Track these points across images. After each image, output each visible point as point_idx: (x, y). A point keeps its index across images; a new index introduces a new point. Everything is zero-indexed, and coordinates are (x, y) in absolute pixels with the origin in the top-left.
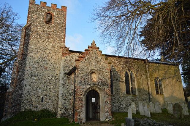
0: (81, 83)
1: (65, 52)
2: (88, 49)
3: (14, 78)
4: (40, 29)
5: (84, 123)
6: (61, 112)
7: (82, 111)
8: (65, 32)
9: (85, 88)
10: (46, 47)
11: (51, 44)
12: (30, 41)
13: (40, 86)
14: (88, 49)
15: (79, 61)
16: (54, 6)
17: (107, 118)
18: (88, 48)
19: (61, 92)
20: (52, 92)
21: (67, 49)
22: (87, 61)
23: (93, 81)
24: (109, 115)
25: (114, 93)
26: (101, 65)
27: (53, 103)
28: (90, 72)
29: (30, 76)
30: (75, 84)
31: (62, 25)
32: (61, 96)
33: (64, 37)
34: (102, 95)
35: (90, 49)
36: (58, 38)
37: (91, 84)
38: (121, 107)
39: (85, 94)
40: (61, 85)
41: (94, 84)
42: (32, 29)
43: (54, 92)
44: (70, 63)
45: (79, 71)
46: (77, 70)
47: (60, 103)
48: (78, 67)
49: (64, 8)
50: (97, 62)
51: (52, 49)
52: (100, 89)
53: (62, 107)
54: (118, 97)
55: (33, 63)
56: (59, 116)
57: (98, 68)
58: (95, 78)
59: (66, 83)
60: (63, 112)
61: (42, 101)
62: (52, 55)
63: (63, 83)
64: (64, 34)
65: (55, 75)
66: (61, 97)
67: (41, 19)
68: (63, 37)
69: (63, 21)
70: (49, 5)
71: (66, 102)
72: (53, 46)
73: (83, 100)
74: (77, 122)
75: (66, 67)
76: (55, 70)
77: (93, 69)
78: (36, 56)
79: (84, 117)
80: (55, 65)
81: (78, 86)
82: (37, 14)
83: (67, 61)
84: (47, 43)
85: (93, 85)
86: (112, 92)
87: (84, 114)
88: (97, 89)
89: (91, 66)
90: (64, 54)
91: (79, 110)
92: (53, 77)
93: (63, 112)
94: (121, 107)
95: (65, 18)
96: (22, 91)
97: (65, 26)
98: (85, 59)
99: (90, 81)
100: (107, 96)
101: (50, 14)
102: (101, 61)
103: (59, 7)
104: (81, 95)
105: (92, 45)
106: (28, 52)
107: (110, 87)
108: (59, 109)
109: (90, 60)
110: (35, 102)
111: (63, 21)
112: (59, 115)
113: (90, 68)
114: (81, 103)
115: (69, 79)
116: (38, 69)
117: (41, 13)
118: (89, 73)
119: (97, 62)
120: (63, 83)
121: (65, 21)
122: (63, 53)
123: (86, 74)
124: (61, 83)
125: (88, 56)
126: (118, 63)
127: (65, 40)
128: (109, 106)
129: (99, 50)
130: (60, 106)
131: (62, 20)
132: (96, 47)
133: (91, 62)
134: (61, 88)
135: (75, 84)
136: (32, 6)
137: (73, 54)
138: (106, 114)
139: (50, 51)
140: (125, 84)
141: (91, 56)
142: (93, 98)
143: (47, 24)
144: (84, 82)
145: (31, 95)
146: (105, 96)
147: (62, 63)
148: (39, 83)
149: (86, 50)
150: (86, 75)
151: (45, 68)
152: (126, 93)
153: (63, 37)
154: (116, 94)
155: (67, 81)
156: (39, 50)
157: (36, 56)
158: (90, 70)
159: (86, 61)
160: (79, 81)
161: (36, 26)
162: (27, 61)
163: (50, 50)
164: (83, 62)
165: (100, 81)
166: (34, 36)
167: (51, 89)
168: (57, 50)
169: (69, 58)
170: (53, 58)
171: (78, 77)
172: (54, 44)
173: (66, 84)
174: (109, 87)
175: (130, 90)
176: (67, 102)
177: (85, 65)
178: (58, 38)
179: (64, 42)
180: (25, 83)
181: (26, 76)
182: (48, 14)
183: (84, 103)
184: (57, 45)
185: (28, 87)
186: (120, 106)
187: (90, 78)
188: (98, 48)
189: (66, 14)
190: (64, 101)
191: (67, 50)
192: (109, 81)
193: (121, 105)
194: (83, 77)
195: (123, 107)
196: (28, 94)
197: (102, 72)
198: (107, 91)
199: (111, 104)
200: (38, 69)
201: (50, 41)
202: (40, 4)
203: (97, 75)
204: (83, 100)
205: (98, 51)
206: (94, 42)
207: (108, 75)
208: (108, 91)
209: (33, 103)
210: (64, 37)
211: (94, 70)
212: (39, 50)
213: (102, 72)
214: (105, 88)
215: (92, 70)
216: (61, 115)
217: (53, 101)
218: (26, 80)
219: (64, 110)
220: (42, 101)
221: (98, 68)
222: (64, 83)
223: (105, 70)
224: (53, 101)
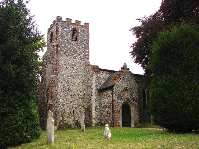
0: (118, 98)
2: (121, 69)
3: (52, 92)
6: (95, 122)
8: (88, 49)
9: (121, 102)
10: (74, 63)
11: (78, 60)
12: (60, 57)
13: (71, 100)
14: (121, 69)
16: (78, 22)
18: (121, 68)
22: (121, 80)
24: (138, 123)
29: (63, 91)
30: (112, 99)
31: (86, 42)
32: (95, 108)
34: (132, 108)
35: (123, 70)
41: (127, 99)
42: (61, 46)
43: (83, 106)
44: (100, 81)
46: (114, 88)
48: (116, 85)
49: (87, 25)
53: (96, 118)
55: (64, 78)
57: (130, 86)
58: (127, 95)
61: (73, 114)
65: (82, 90)
67: (67, 34)
69: (86, 38)
70: (73, 21)
71: (99, 114)
73: (121, 111)
75: (97, 83)
76: (82, 85)
77: (126, 87)
78: (66, 72)
81: (117, 100)
84: (75, 60)
95: (88, 35)
96: (57, 104)
97: (88, 43)
99: (124, 97)
101: (75, 30)
103: (82, 24)
104: (118, 107)
105: (124, 66)
106: (59, 68)
108: (93, 120)
110: (68, 114)
113: (124, 86)
114: (119, 114)
116: (68, 84)
117: (67, 30)
118: (123, 90)
121: (88, 38)
124: (94, 98)
125: (122, 76)
127: (89, 56)
135: (112, 99)
136: (60, 23)
137: (101, 72)
140: (142, 100)
141: (124, 76)
145: (64, 108)
148: (70, 97)
151: (74, 83)
153: (87, 54)
156: (68, 66)
157: (66, 72)
160: (117, 97)
161: (64, 42)
162: (59, 76)
166: (63, 53)
167: (80, 103)
168: (82, 66)
169: (99, 76)
170: (81, 74)
171: (116, 93)
172: (80, 60)
179: (88, 59)
180: (58, 96)
181: (59, 91)
182: (74, 30)
183: (121, 113)
184: (83, 62)
185: (62, 100)
188: (128, 69)
189: (88, 31)
196: (62, 107)
200: (68, 84)
201: (76, 57)
202: (65, 21)
203: (129, 92)
206: (126, 65)
209: (67, 115)
212: (68, 66)
216: (95, 124)
218: (59, 94)
219: (97, 121)
220: (73, 114)
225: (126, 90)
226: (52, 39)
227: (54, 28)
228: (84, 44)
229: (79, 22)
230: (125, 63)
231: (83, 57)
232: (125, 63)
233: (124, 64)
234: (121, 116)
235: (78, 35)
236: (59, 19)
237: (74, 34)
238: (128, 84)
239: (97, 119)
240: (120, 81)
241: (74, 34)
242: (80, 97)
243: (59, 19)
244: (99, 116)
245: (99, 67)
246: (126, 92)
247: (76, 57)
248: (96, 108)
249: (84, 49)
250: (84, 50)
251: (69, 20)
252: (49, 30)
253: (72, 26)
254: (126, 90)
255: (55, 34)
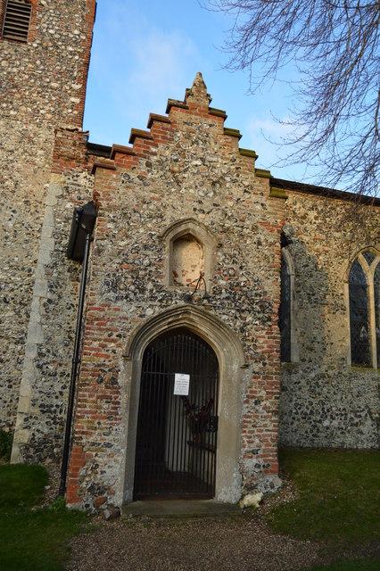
0: (114, 286)
1: (68, 150)
5: (116, 515)
7: (108, 445)
9: (132, 314)
11: (18, 126)
15: (113, 169)
17: (251, 488)
18: (170, 107)
19: (34, 339)
20: (8, 338)
21: (76, 137)
22: (155, 174)
23: (185, 283)
24: (266, 469)
25: (295, 358)
26: (230, 203)
27: (10, 387)
28: (171, 235)
31: (70, 49)
33: (77, 101)
34: (230, 361)
35: (178, 115)
36: (51, 101)
37: (170, 296)
38: (326, 423)
39: (133, 347)
40: (36, 304)
41: (189, 299)
45: (110, 225)
47: (26, 390)
48: (104, 204)
50: (214, 184)
51: (21, 150)
52: (217, 324)
53: (37, 411)
54: (313, 375)
56: (16, 456)
59: (60, 297)
60: (38, 435)
62: (18, 175)
63: (49, 295)
64: (79, 86)
65: (27, 262)
66: (35, 360)
68: (73, 99)
69: (76, 32)
71: (57, 388)
72: (25, 137)
73: (123, 379)
74: (79, 506)
76: (27, 242)
79: (120, 479)
80: (29, 219)
81: (99, 301)
83: (74, 196)
85: (182, 303)
86: (285, 353)
87: (121, 458)
88: (204, 329)
89: (177, 203)
90: (61, 160)
91: (91, 439)
92: (19, 273)
93: (38, 435)
94: (326, 423)
98: (149, 165)
99: (165, 282)
100: (256, 367)
102: (234, 181)
105: (187, 95)
107: (275, 318)
108: (20, 421)
109: (173, 172)
111: (76, 32)
112: (15, 450)
113: (169, 214)
114: (108, 399)
115: (78, 280)
118: (160, 238)
119: (214, 184)
120: (49, 295)
122: (58, 156)
123: (144, 239)
124: (41, 291)
125: (163, 151)
126: (316, 218)
128: (268, 422)
129: (227, 124)
130: (24, 406)
131: (76, 28)
132: (210, 109)
133: (178, 182)
134: (36, 317)
138: (250, 463)
139: (10, 158)
140: (347, 320)
141: (183, 153)
142: (178, 376)
143: (6, 42)
144: (136, 282)
146: (247, 366)
147: (51, 200)
149: (154, 119)
150: (146, 247)
152: (353, 359)
153: (73, 99)
154: (303, 360)
155: (70, 288)
158: (168, 223)
159: (149, 175)
160: (102, 278)
163: (12, 151)
164: (133, 175)
165: (222, 282)
169: (82, 181)
170: (25, 187)
173: (63, 303)
174: (269, 319)
175: (369, 345)
176: (64, 387)
177: (146, 193)
178: (51, 101)
183: (124, 398)
186: (320, 422)
187: (166, 264)
190: (44, 384)
191: (74, 145)
192: (272, 288)
193: (324, 417)
194: (131, 256)
195: (335, 423)
197: (235, 238)
198: (261, 341)
199: (276, 413)
201: (12, 112)
203: (209, 249)
204: (123, 379)
205: (216, 130)
206: (201, 85)
207: (266, 257)
208: (265, 339)
210: (77, 101)
211: (190, 225)
213: (235, 238)
214: (245, 325)
215: (179, 223)
216: (27, 447)
217: (9, 381)
219: (43, 427)
221: (216, 216)
222: (54, 297)
223: (255, 228)
224: (9, 381)
228: (61, 58)
231: (49, 112)
234: (123, 411)
235: (34, 15)
238: (207, 205)
239: (45, 419)
240: (141, 178)
242: (11, 295)
244: (55, 402)
245: (91, 141)
247: (12, 112)
248: (41, 355)
249: (58, 80)
250: (53, 84)
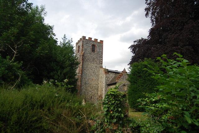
4: (89, 55)
13: (90, 90)
35: (123, 73)
49: (102, 41)
70: (93, 40)
82: (87, 46)
97: (102, 54)
103: (99, 41)
121: (102, 50)
122: (105, 73)
124: (104, 90)
136: (84, 41)
137: (110, 73)
148: (89, 88)
151: (92, 80)
179: (102, 64)
180: (82, 87)
181: (83, 84)
184: (98, 66)
185: (84, 90)
189: (103, 46)
225: (124, 85)
226: (79, 50)
227: (81, 44)
229: (97, 40)
230: (125, 69)
232: (125, 69)
233: (124, 69)
236: (84, 37)
237: (94, 47)
241: (94, 47)
243: (84, 37)
246: (124, 86)
251: (90, 39)
252: (77, 43)
253: (92, 42)
254: (124, 85)
255: (81, 48)
